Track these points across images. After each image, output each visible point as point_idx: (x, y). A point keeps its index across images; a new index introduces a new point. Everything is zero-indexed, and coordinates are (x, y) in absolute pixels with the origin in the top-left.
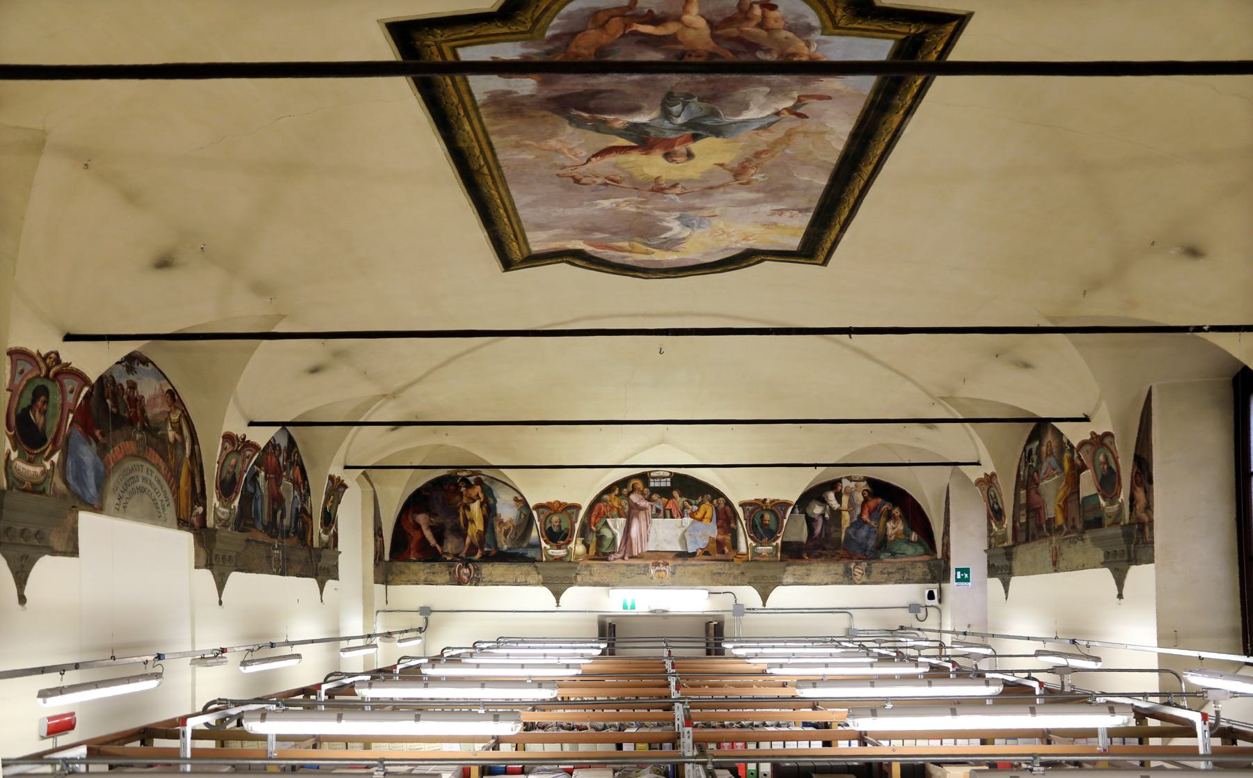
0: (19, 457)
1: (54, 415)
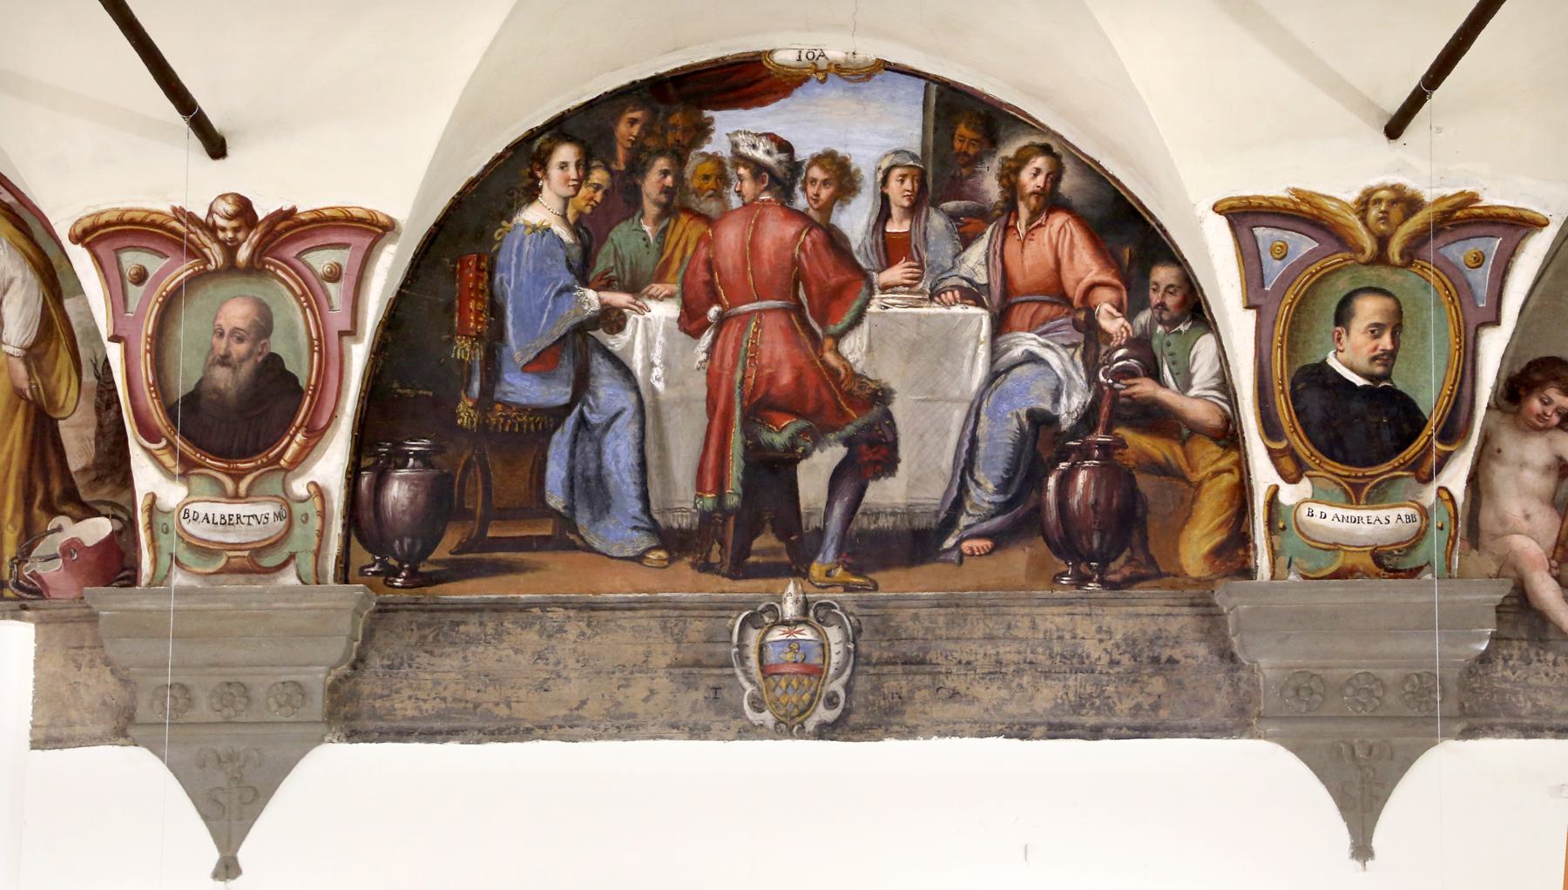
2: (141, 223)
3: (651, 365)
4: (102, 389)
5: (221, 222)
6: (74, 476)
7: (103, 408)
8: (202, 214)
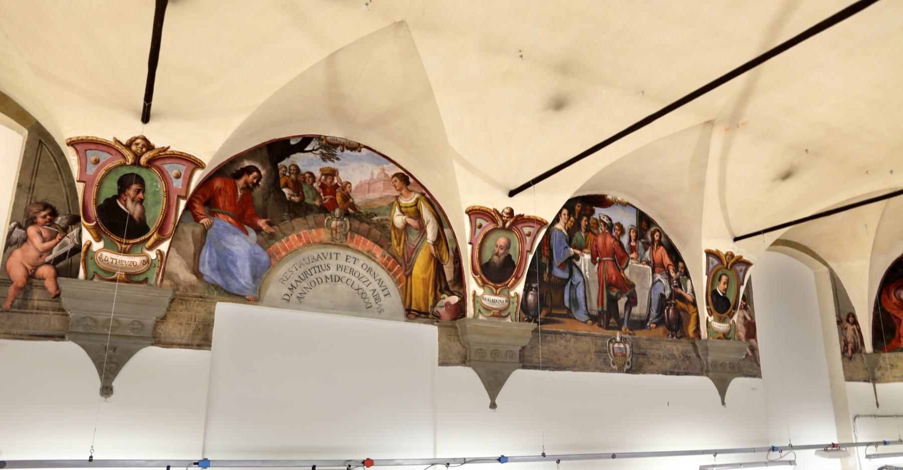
0: (106, 247)
1: (157, 203)
2: (484, 211)
3: (585, 271)
5: (504, 215)
8: (500, 211)
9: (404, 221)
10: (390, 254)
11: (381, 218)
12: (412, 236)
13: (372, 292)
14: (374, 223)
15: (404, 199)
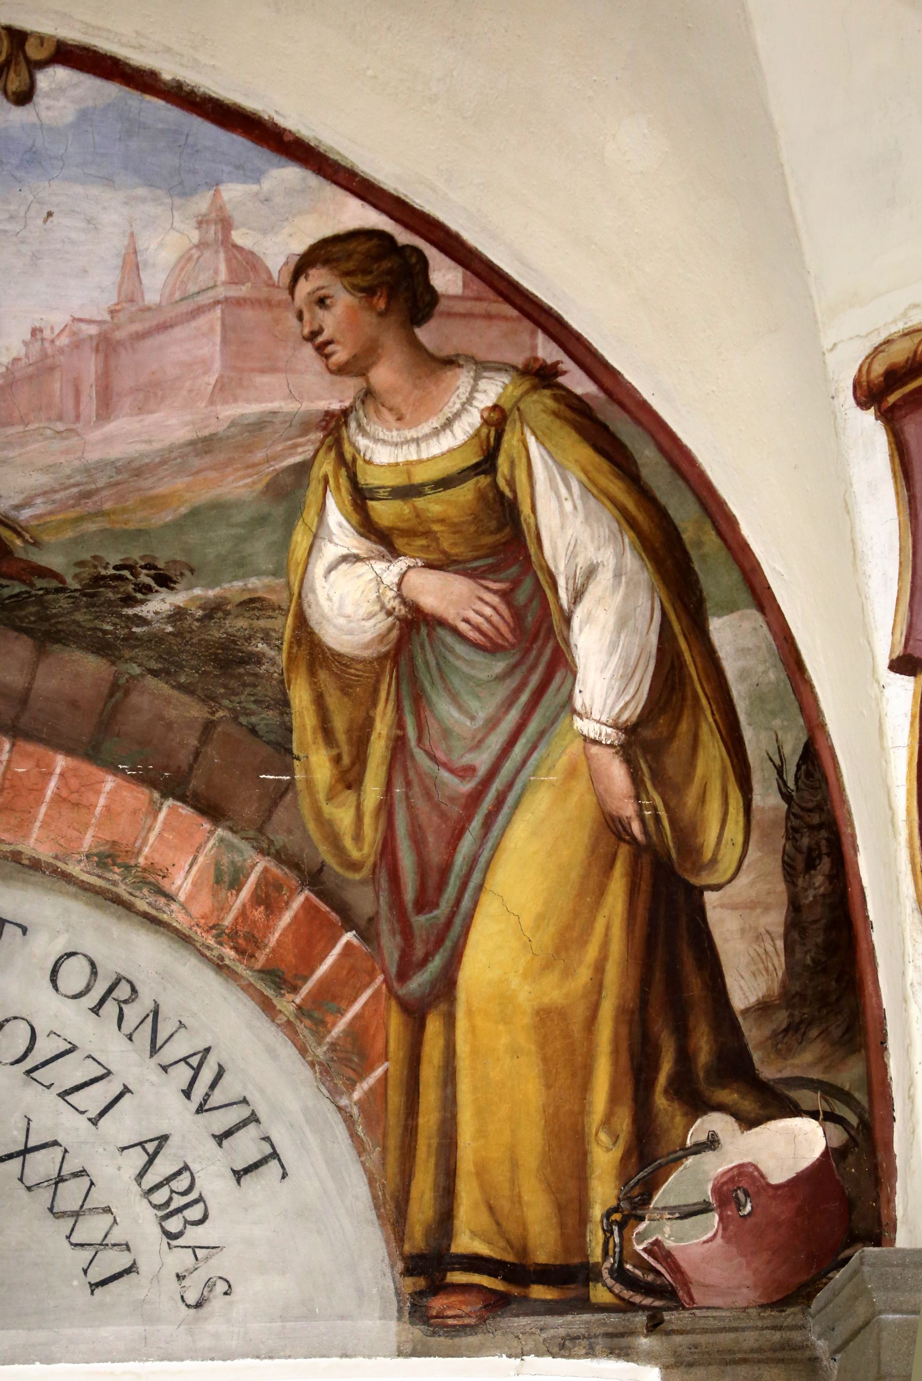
4: (796, 823)
6: (740, 1019)
7: (800, 865)
9: (392, 603)
10: (281, 857)
11: (211, 593)
12: (455, 698)
13: (138, 1158)
14: (157, 640)
15: (394, 435)
